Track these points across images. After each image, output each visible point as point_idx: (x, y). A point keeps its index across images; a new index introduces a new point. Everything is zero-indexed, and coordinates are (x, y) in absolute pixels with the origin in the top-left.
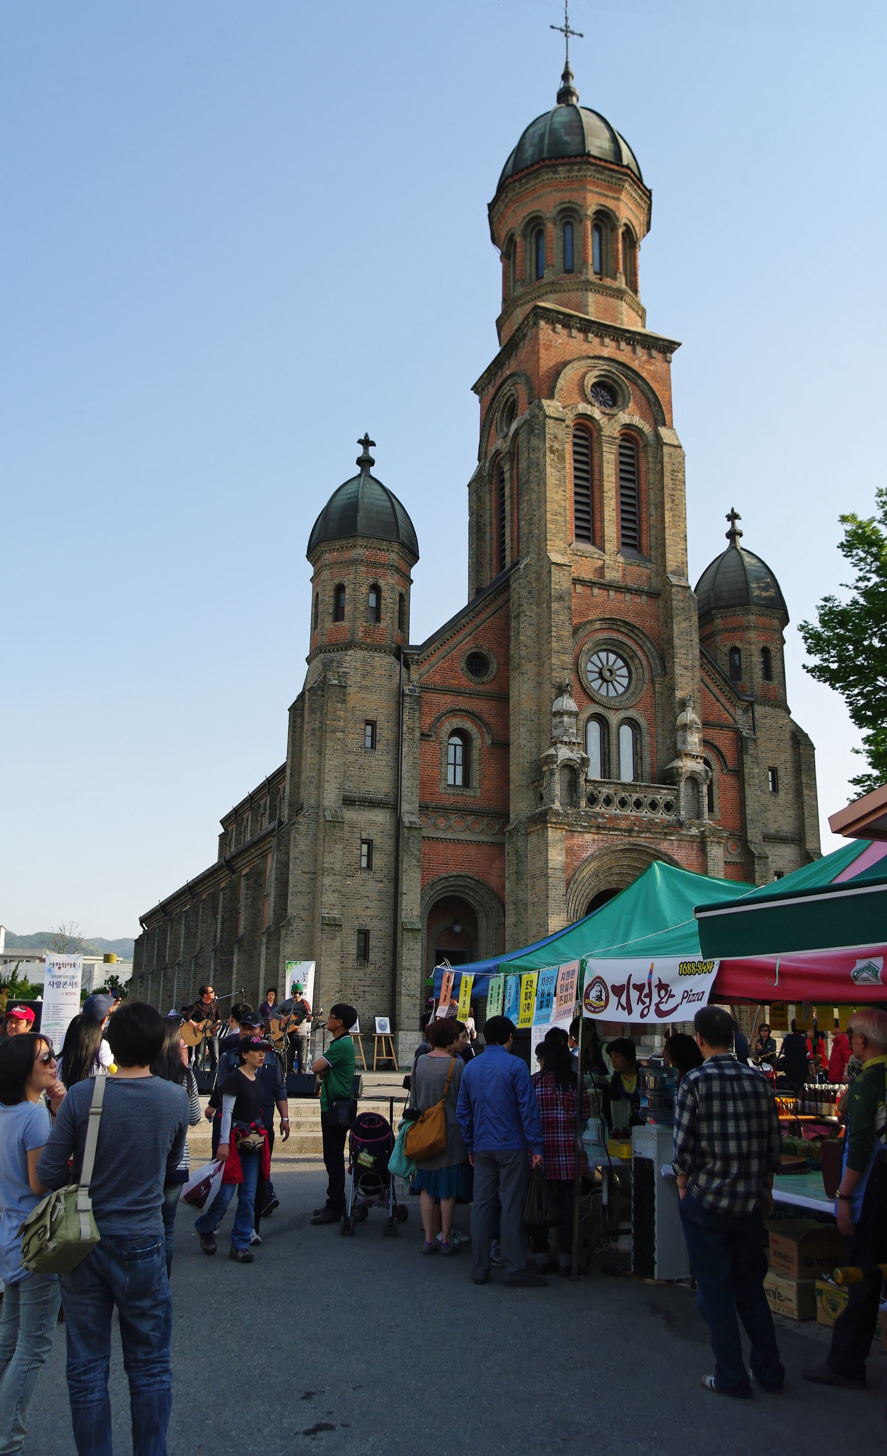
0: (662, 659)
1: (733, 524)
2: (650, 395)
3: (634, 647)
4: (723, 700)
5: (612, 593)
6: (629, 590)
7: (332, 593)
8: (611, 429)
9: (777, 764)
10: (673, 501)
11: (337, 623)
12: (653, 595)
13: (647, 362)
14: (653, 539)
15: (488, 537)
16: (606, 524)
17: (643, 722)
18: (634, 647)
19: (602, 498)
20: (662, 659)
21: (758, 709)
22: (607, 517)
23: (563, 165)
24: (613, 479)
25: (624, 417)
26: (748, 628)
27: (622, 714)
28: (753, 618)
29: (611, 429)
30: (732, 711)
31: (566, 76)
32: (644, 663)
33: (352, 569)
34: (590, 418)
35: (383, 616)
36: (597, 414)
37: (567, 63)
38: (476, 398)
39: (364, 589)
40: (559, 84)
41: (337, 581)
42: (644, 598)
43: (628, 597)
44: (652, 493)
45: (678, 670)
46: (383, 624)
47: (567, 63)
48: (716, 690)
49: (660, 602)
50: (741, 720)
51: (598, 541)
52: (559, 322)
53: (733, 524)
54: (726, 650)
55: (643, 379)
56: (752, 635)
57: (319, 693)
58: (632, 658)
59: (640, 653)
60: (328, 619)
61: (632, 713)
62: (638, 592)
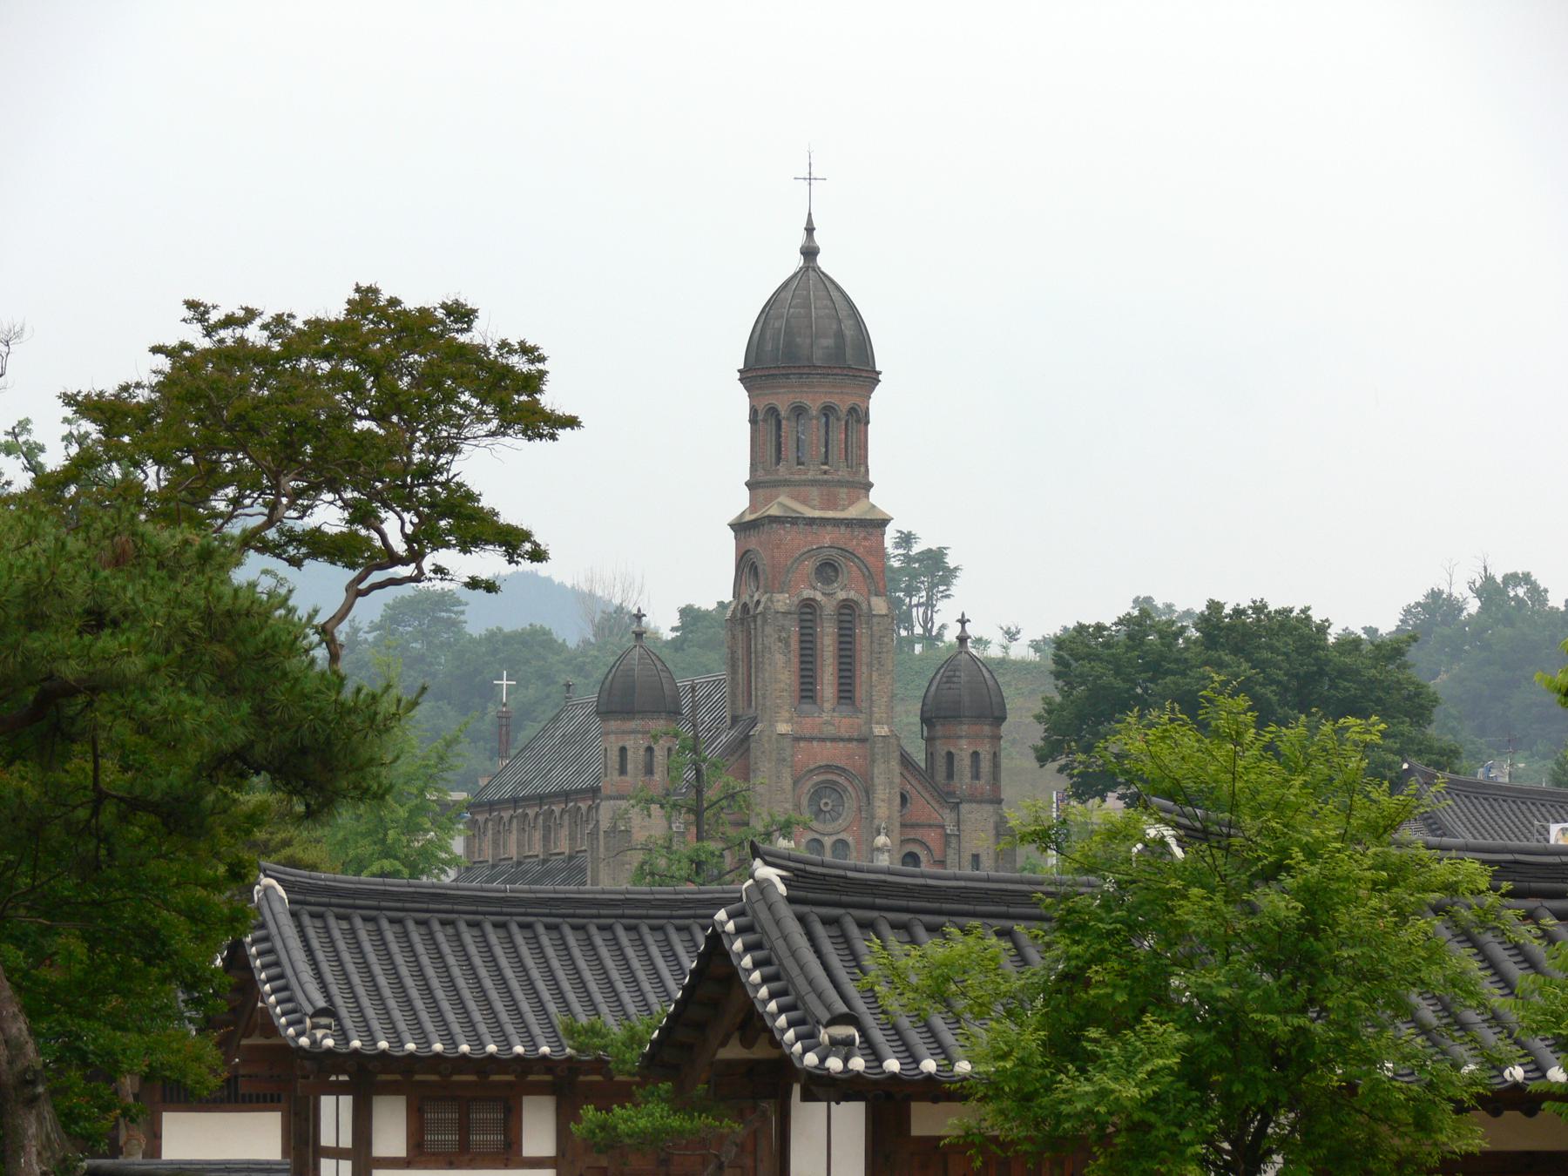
0: (867, 793)
1: (963, 627)
2: (865, 570)
3: (846, 784)
4: (933, 803)
5: (829, 744)
6: (842, 740)
7: (617, 753)
8: (829, 606)
9: (980, 851)
10: (879, 662)
11: (623, 777)
12: (862, 740)
13: (865, 538)
14: (864, 692)
15: (740, 670)
16: (825, 687)
17: (850, 840)
18: (846, 784)
19: (822, 665)
20: (867, 793)
21: (964, 808)
22: (825, 681)
23: (794, 374)
24: (831, 648)
25: (841, 595)
26: (960, 737)
27: (834, 838)
28: (965, 727)
29: (829, 606)
30: (940, 811)
31: (810, 230)
32: (853, 795)
33: (632, 736)
34: (813, 600)
35: (655, 771)
36: (819, 597)
37: (810, 214)
38: (732, 534)
39: (642, 752)
40: (800, 238)
41: (620, 744)
42: (855, 743)
43: (841, 745)
44: (864, 654)
45: (877, 803)
46: (657, 777)
47: (810, 214)
48: (927, 796)
49: (868, 745)
50: (948, 817)
51: (819, 701)
52: (788, 522)
53: (963, 627)
54: (944, 753)
55: (858, 558)
56: (964, 743)
57: (612, 835)
58: (844, 791)
59: (850, 789)
60: (616, 773)
61: (843, 836)
62: (850, 740)
